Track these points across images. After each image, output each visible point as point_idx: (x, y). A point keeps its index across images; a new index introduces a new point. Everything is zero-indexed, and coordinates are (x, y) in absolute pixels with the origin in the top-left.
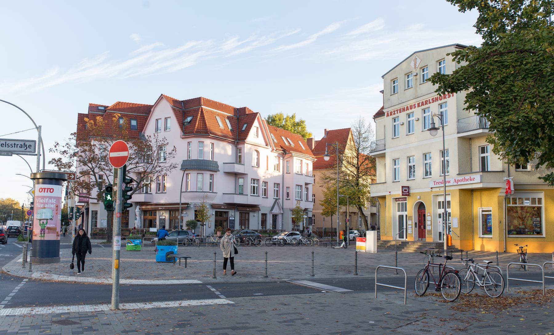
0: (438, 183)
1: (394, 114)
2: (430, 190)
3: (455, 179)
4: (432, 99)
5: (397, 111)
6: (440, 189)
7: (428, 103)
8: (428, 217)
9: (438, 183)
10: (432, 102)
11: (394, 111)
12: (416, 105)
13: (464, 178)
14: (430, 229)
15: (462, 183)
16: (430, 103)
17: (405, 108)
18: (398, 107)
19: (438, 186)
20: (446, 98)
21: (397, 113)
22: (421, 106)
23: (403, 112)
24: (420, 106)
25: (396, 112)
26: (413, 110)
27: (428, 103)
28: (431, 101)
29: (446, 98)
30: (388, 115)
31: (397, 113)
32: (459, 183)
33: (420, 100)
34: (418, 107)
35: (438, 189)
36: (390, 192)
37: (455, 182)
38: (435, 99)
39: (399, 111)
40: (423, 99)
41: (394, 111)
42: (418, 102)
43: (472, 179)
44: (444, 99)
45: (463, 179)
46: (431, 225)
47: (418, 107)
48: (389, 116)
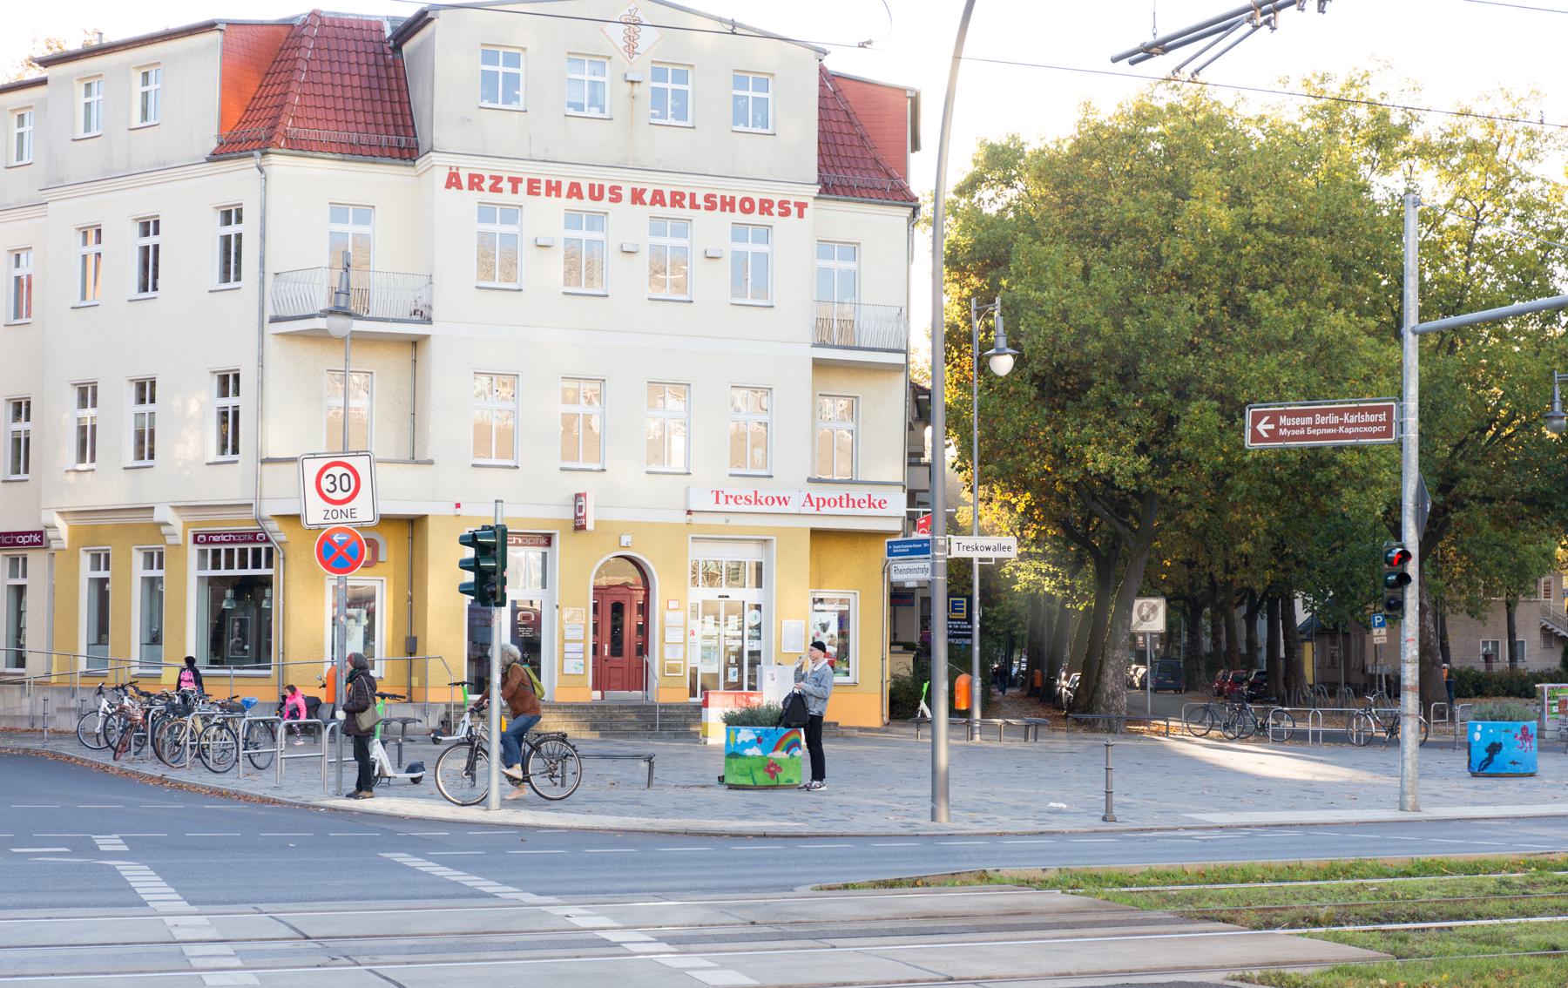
0: (731, 501)
1: (495, 189)
2: (684, 518)
3: (809, 496)
4: (707, 198)
5: (515, 182)
6: (727, 521)
7: (686, 202)
8: (669, 615)
9: (731, 501)
10: (707, 208)
11: (498, 179)
12: (626, 194)
13: (845, 497)
14: (680, 656)
15: (837, 510)
16: (694, 206)
17: (559, 184)
18: (526, 171)
19: (732, 507)
20: (771, 214)
21: (515, 190)
22: (653, 203)
23: (548, 194)
24: (643, 203)
25: (506, 185)
26: (604, 204)
27: (686, 202)
28: (700, 200)
29: (771, 214)
30: (453, 181)
31: (515, 190)
32: (826, 510)
33: (650, 183)
34: (634, 202)
35: (719, 520)
36: (458, 506)
37: (808, 504)
38: (718, 201)
39: (523, 187)
40: (668, 185)
41: (498, 179)
42: (639, 187)
43: (876, 504)
44: (761, 213)
45: (841, 498)
46: (564, 641)
47: (634, 202)
48: (460, 187)
